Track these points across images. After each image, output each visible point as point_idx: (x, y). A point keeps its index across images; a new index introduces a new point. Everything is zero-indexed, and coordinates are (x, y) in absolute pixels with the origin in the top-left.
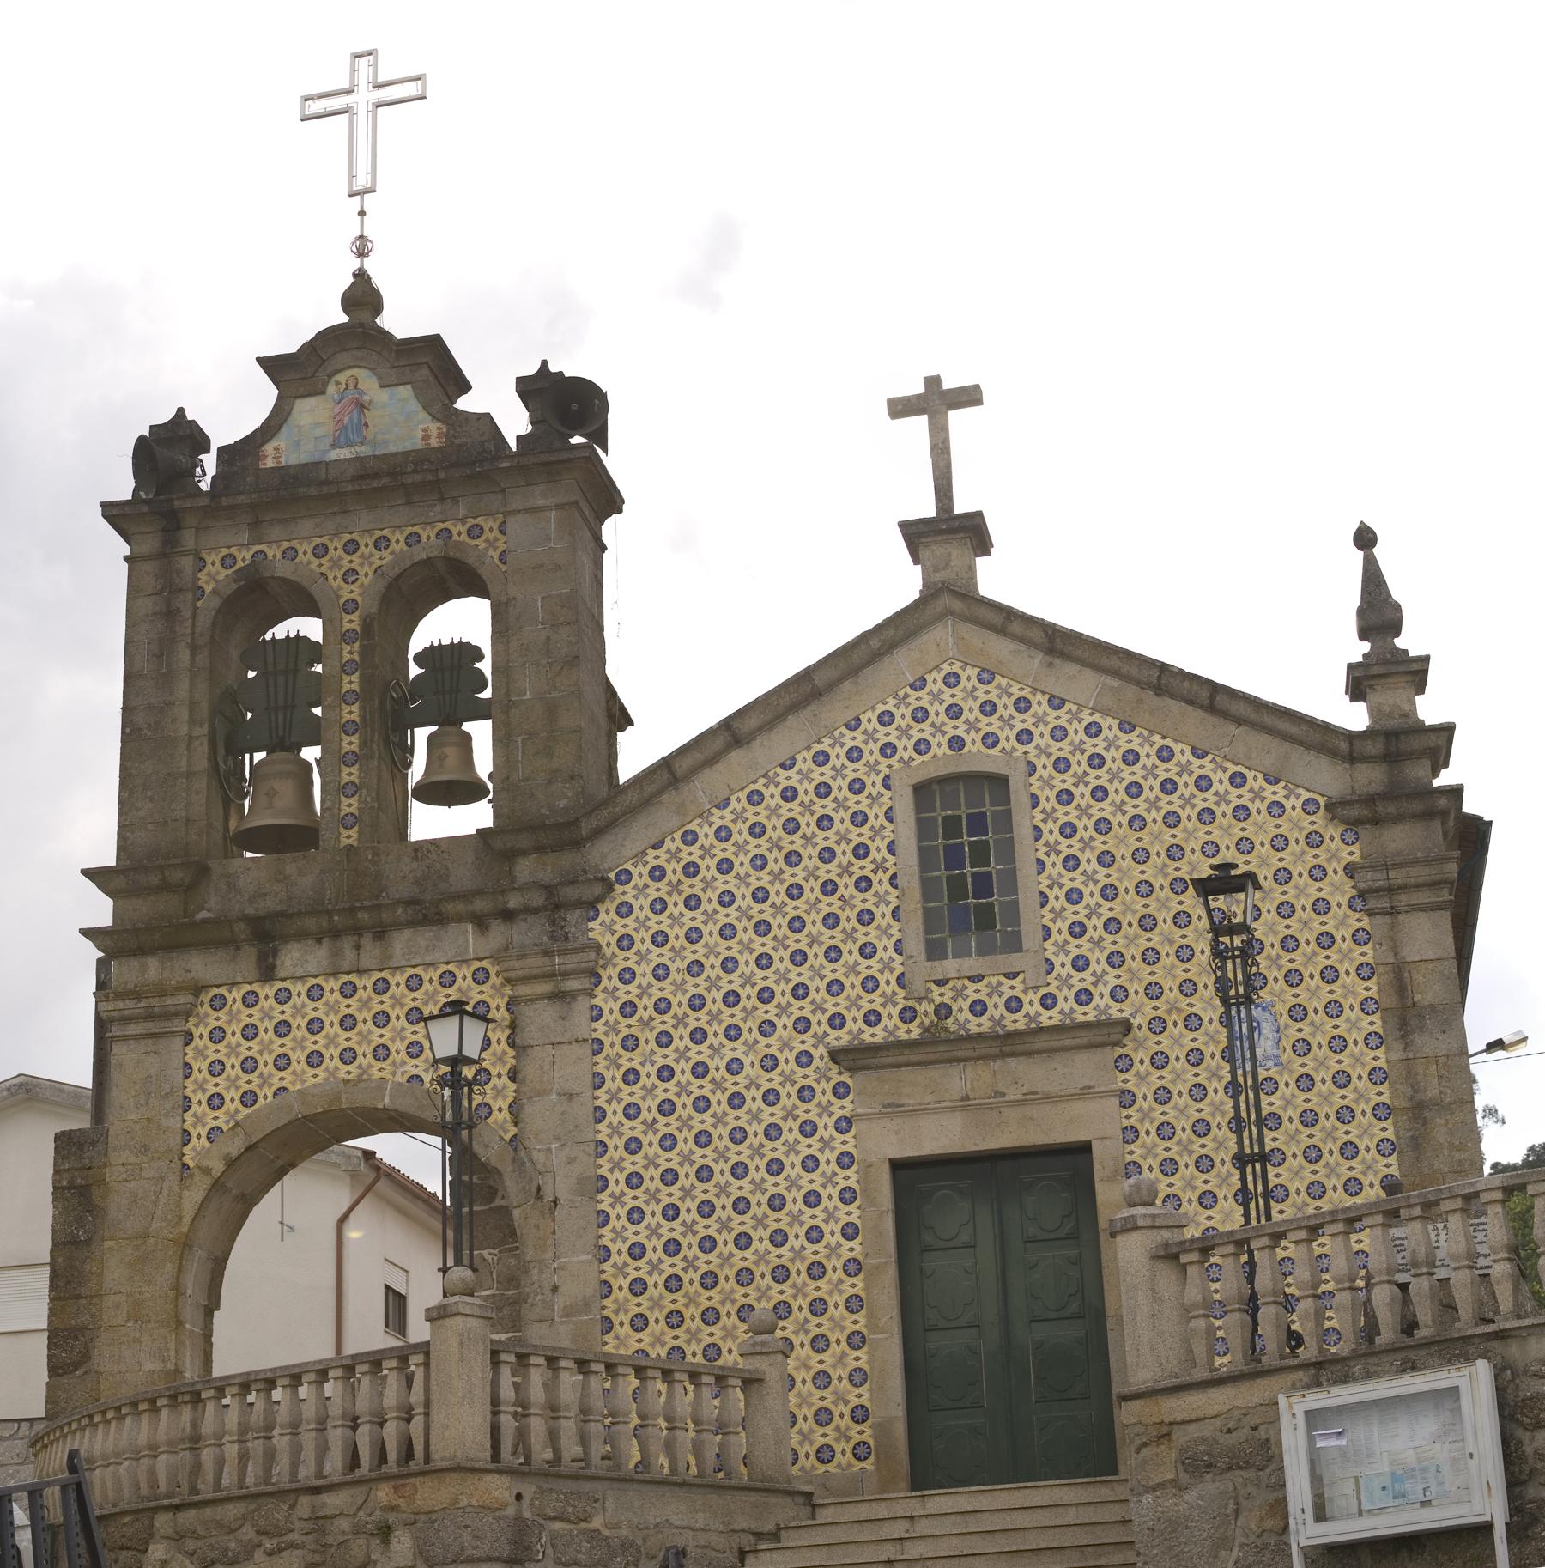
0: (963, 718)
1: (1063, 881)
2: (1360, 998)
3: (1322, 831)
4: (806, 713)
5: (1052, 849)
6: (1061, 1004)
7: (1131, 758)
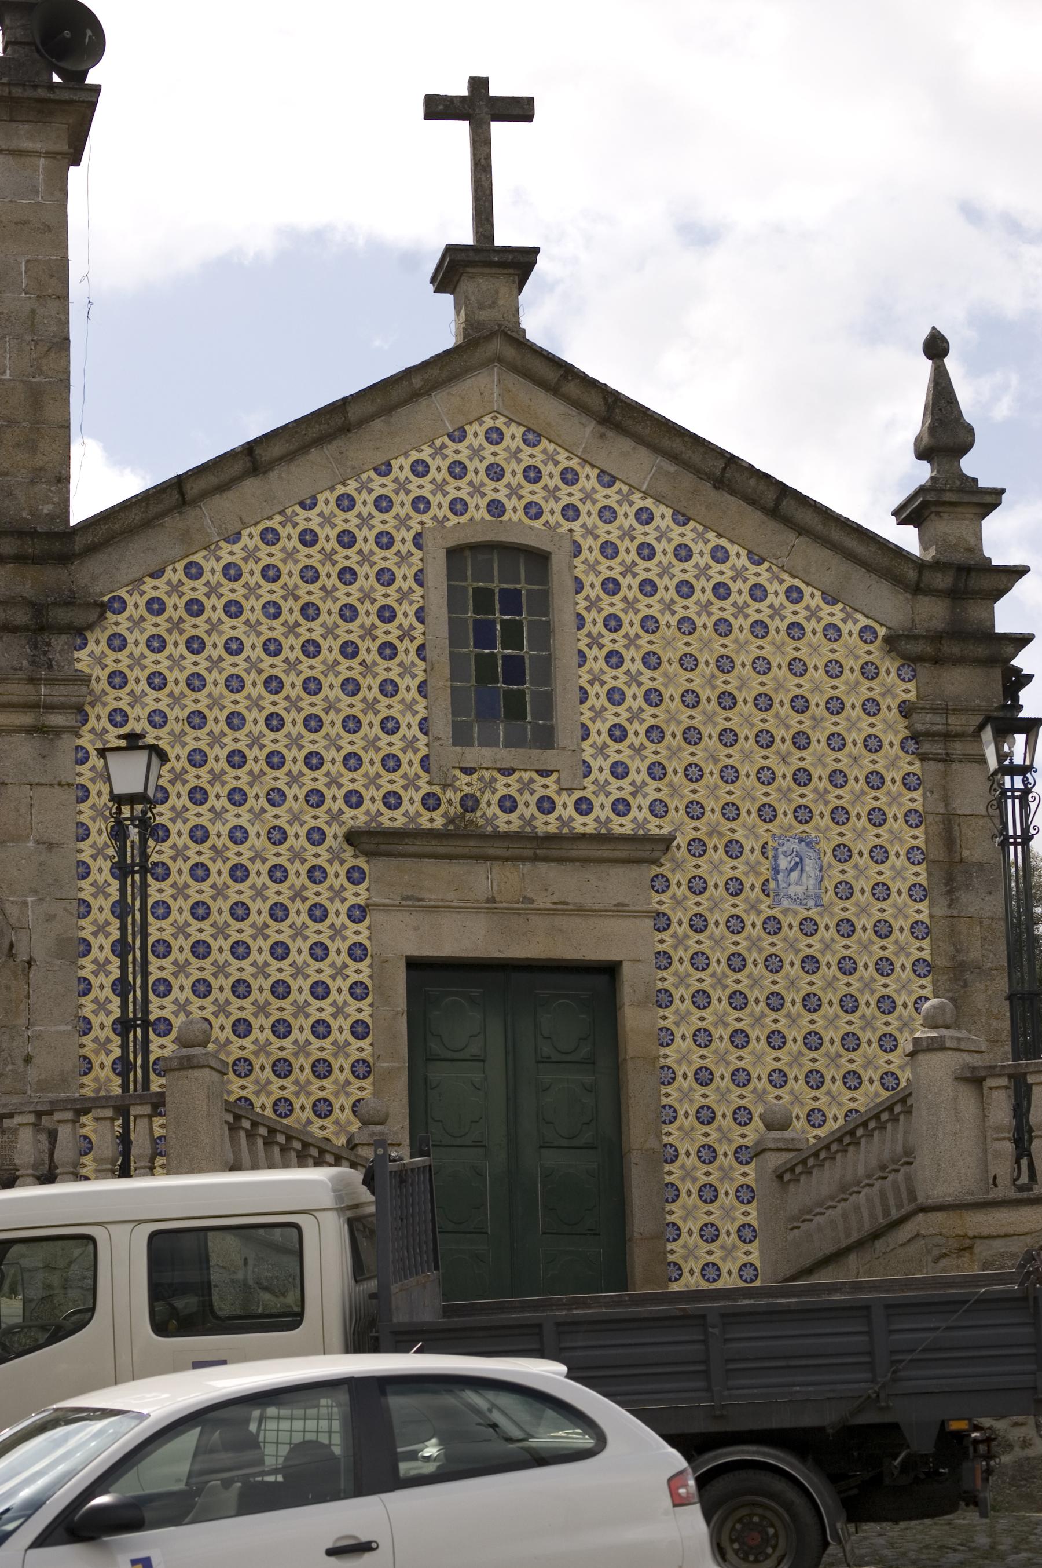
0: (505, 481)
1: (605, 678)
2: (907, 846)
3: (878, 663)
4: (331, 449)
5: (595, 641)
6: (597, 811)
7: (683, 553)
